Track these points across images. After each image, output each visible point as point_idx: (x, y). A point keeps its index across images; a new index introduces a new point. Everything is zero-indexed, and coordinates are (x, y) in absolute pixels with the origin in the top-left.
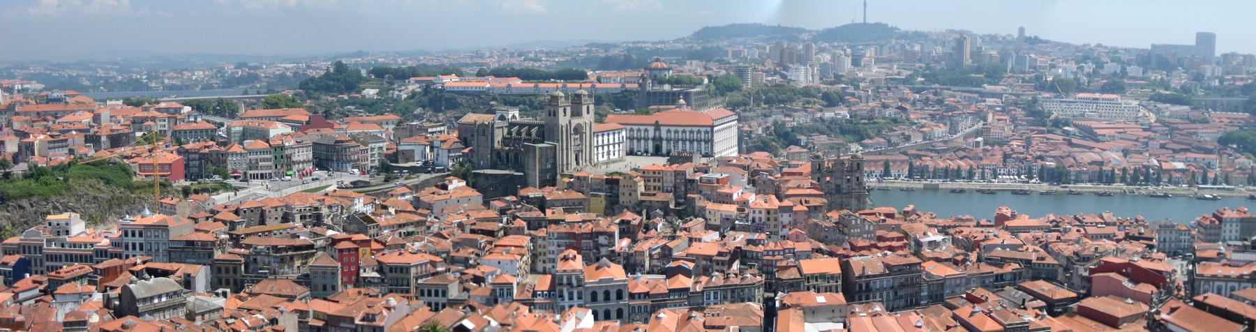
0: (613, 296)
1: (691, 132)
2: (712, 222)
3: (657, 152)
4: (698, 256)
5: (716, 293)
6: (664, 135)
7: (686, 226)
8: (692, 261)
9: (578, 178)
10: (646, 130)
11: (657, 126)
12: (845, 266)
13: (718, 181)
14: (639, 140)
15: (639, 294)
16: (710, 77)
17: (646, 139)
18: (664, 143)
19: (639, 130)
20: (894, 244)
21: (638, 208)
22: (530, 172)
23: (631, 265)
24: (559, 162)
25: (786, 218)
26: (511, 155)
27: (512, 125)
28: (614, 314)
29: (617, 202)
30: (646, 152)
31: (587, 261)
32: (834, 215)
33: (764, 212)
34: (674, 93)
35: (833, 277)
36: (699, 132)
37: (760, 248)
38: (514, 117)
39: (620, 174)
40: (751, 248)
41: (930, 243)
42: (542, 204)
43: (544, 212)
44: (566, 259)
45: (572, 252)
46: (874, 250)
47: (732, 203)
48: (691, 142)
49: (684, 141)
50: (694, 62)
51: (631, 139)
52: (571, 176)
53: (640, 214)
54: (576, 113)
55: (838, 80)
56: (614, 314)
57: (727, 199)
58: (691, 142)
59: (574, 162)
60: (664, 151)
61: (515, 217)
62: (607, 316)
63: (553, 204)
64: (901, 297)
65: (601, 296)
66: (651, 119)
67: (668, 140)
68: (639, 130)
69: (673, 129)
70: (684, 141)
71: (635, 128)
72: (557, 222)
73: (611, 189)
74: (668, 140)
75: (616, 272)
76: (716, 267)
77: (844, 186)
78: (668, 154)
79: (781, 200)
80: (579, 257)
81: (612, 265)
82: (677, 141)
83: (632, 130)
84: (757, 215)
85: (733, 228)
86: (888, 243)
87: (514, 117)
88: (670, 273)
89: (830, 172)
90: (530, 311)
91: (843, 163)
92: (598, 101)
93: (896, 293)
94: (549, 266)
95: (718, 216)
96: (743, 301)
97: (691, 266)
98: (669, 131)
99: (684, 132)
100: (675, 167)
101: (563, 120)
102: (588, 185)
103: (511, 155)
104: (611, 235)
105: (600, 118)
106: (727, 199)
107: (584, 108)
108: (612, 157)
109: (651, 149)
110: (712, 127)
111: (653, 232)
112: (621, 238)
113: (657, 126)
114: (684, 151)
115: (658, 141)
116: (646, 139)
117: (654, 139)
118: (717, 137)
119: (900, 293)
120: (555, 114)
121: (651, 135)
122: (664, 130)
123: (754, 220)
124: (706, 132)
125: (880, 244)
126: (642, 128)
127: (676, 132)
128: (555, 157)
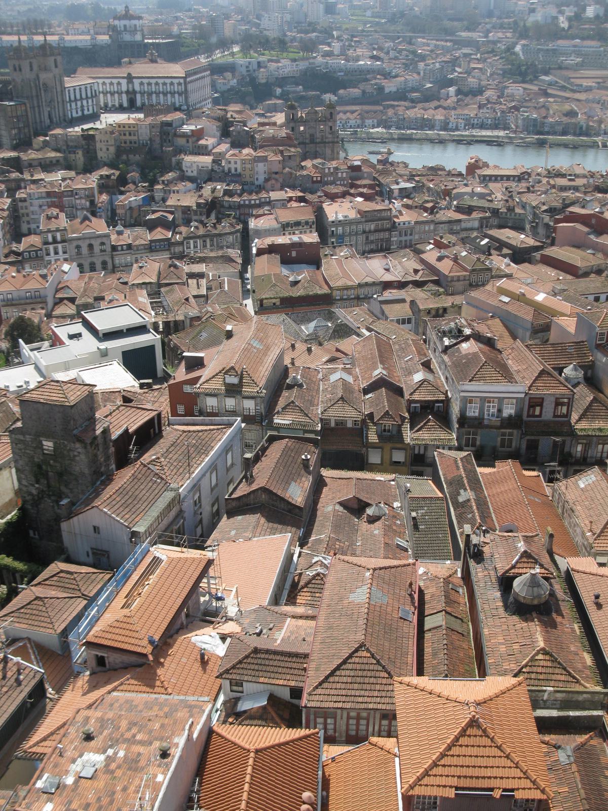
0: (97, 249)
1: (165, 84)
2: (189, 174)
3: (132, 107)
5: (195, 242)
6: (137, 88)
8: (171, 213)
10: (119, 84)
12: (320, 213)
14: (112, 94)
15: (122, 246)
18: (138, 97)
19: (111, 84)
20: (365, 190)
23: (112, 221)
25: (261, 167)
28: (99, 266)
29: (96, 157)
30: (121, 106)
31: (71, 217)
32: (308, 163)
33: (239, 162)
35: (307, 223)
37: (236, 199)
39: (97, 129)
40: (226, 198)
41: (400, 189)
42: (16, 164)
43: (22, 173)
44: (49, 218)
45: (55, 211)
46: (347, 196)
47: (208, 154)
48: (165, 94)
49: (158, 94)
55: (312, 27)
56: (99, 266)
59: (48, 121)
60: (139, 103)
62: (93, 268)
63: (31, 165)
64: (372, 242)
65: (85, 250)
66: (122, 72)
68: (111, 84)
69: (146, 81)
72: (35, 182)
73: (88, 145)
75: (99, 226)
76: (194, 217)
77: (318, 135)
79: (255, 149)
80: (62, 216)
81: (93, 219)
82: (150, 94)
83: (104, 83)
84: (233, 166)
85: (210, 179)
86: (361, 190)
88: (151, 226)
89: (302, 121)
90: (18, 271)
91: (316, 112)
93: (367, 238)
94: (33, 226)
95: (195, 168)
96: (222, 248)
97: (170, 217)
98: (142, 84)
99: (157, 84)
100: (150, 120)
106: (203, 151)
108: (86, 112)
109: (125, 104)
111: (131, 186)
113: (130, 78)
114: (159, 103)
115: (132, 94)
117: (127, 92)
119: (372, 238)
121: (124, 88)
123: (229, 169)
124: (179, 84)
125: (352, 191)
127: (149, 84)
128: (27, 115)
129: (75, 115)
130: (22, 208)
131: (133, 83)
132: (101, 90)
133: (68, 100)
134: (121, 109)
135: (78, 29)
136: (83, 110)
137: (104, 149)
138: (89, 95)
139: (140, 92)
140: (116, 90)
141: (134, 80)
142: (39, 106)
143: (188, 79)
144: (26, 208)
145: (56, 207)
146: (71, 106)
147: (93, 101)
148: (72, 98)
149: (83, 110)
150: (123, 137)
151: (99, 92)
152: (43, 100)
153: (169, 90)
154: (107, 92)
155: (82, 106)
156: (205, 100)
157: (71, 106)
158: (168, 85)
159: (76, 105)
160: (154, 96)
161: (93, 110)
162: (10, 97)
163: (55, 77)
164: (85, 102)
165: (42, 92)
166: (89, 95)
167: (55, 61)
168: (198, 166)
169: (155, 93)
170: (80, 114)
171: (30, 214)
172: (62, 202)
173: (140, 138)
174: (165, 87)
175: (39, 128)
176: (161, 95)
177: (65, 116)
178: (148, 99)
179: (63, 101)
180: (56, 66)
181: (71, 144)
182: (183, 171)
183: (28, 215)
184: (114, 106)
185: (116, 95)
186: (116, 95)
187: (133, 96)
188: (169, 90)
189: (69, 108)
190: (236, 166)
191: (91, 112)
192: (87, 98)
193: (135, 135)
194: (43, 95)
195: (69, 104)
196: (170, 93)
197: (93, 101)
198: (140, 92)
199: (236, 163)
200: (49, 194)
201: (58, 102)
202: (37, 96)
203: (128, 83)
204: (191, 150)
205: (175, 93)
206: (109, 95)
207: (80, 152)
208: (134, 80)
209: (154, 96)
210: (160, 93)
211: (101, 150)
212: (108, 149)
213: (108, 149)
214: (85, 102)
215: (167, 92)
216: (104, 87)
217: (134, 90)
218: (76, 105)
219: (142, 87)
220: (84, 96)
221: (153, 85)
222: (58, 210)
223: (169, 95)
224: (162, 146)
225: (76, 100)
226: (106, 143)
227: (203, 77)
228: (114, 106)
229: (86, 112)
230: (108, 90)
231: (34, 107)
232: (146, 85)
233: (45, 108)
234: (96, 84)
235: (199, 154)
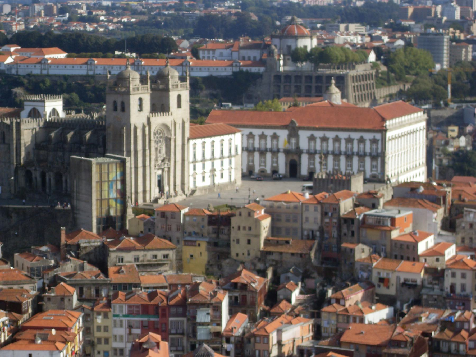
1: (349, 140)
2: (383, 290)
4: (357, 346)
6: (304, 144)
7: (338, 295)
9: (163, 214)
10: (275, 137)
11: (293, 132)
13: (393, 220)
14: (263, 153)
16: (378, 52)
17: (275, 152)
18: (305, 159)
19: (263, 137)
21: (260, 264)
22: (82, 205)
24: (130, 189)
26: (50, 177)
27: (49, 126)
29: (227, 255)
30: (275, 171)
34: (319, 78)
36: (362, 140)
38: (54, 111)
39: (231, 207)
48: (349, 157)
50: (353, 27)
51: (249, 150)
52: (150, 212)
53: (263, 273)
54: (159, 106)
57: (406, 251)
58: (349, 157)
59: (155, 192)
60: (304, 171)
61: (55, 281)
67: (311, 154)
68: (263, 137)
69: (318, 134)
70: (337, 155)
71: (257, 132)
73: (217, 232)
74: (311, 154)
78: (310, 177)
83: (251, 136)
84: (458, 281)
85: (417, 302)
87: (54, 111)
92: (195, 86)
98: (312, 138)
99: (337, 139)
101: (137, 118)
102: (181, 228)
103: (50, 177)
104: (217, 308)
105: (197, 115)
107: (173, 96)
109: (282, 170)
110: (383, 131)
111: (283, 305)
112: (232, 313)
114: (337, 171)
116: (275, 152)
117: (287, 152)
118: (392, 149)
120: (124, 107)
122: (304, 135)
123: (453, 287)
124: (374, 141)
126: (269, 132)
128: (123, 181)
129: (200, 184)
130: (99, 328)
131: (297, 136)
132: (245, 145)
133: (191, 159)
134: (274, 176)
135: (214, 50)
136: (213, 176)
137: (243, 241)
138: (226, 153)
139: (309, 153)
140: (269, 146)
141: (301, 133)
142: (144, 166)
143: (389, 135)
144: (106, 329)
145: (156, 331)
146: (195, 169)
147: (230, 163)
148: (199, 157)
149: (213, 176)
150: (279, 224)
151: (243, 149)
152: (153, 157)
153: (355, 150)
154: (254, 150)
155: (213, 170)
156: (415, 167)
157: (195, 169)
158: (355, 143)
159: (204, 167)
160: (330, 158)
161: (230, 176)
162: (101, 150)
163: (175, 124)
164: (217, 163)
165: (153, 144)
166: (226, 153)
167: (179, 97)
168: (398, 278)
169: (333, 153)
170: (208, 182)
171: (111, 340)
172: (166, 324)
173: (306, 226)
174: (349, 146)
175: (140, 201)
176: (343, 159)
177: (183, 183)
178: (321, 163)
179: (183, 160)
180: (179, 106)
181: (190, 229)
182: (373, 286)
183: (107, 341)
184: (263, 171)
185: (269, 155)
186: (269, 155)
187: (295, 158)
188: (355, 150)
189: (191, 172)
190: (463, 281)
191: (226, 180)
192: (222, 157)
193: (295, 221)
194: (153, 149)
195: (191, 166)
196: (358, 154)
197: (230, 163)
198: (309, 153)
199: (463, 276)
200: (145, 310)
201: (175, 162)
202: (144, 150)
203: (290, 136)
204: (388, 250)
205: (365, 155)
206: (257, 155)
207: (204, 245)
208: (301, 133)
209: (330, 158)
210: (340, 154)
211: (238, 241)
212: (249, 242)
213: (249, 242)
214: (217, 163)
215: (353, 154)
216: (251, 141)
217: (298, 148)
218: (204, 167)
219: (312, 144)
220: (217, 154)
221: (331, 142)
222: (158, 337)
223: (355, 160)
224: (339, 241)
225: (204, 160)
226: (247, 231)
227: (414, 132)
228: (263, 171)
229: (218, 180)
230: (257, 145)
231: (136, 168)
232: (318, 141)
233: (153, 170)
234: (238, 135)
235: (402, 258)
